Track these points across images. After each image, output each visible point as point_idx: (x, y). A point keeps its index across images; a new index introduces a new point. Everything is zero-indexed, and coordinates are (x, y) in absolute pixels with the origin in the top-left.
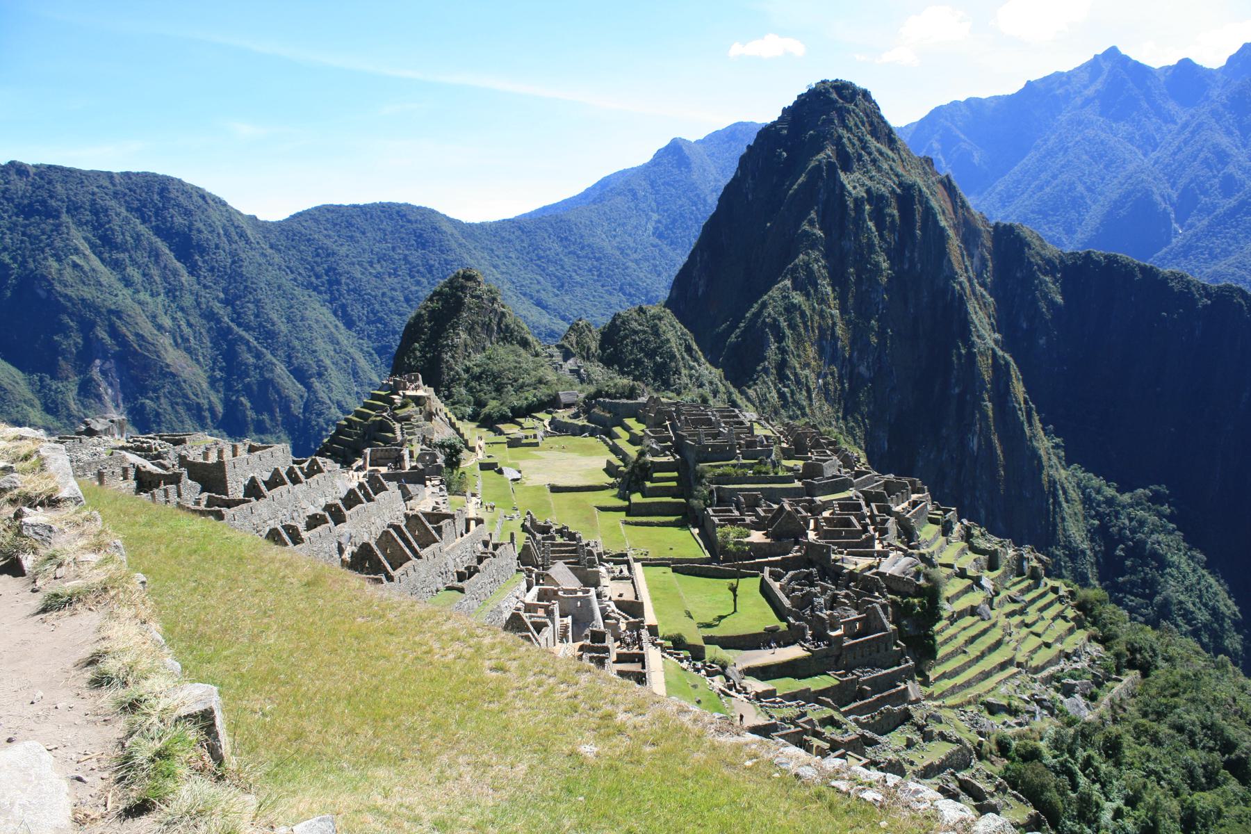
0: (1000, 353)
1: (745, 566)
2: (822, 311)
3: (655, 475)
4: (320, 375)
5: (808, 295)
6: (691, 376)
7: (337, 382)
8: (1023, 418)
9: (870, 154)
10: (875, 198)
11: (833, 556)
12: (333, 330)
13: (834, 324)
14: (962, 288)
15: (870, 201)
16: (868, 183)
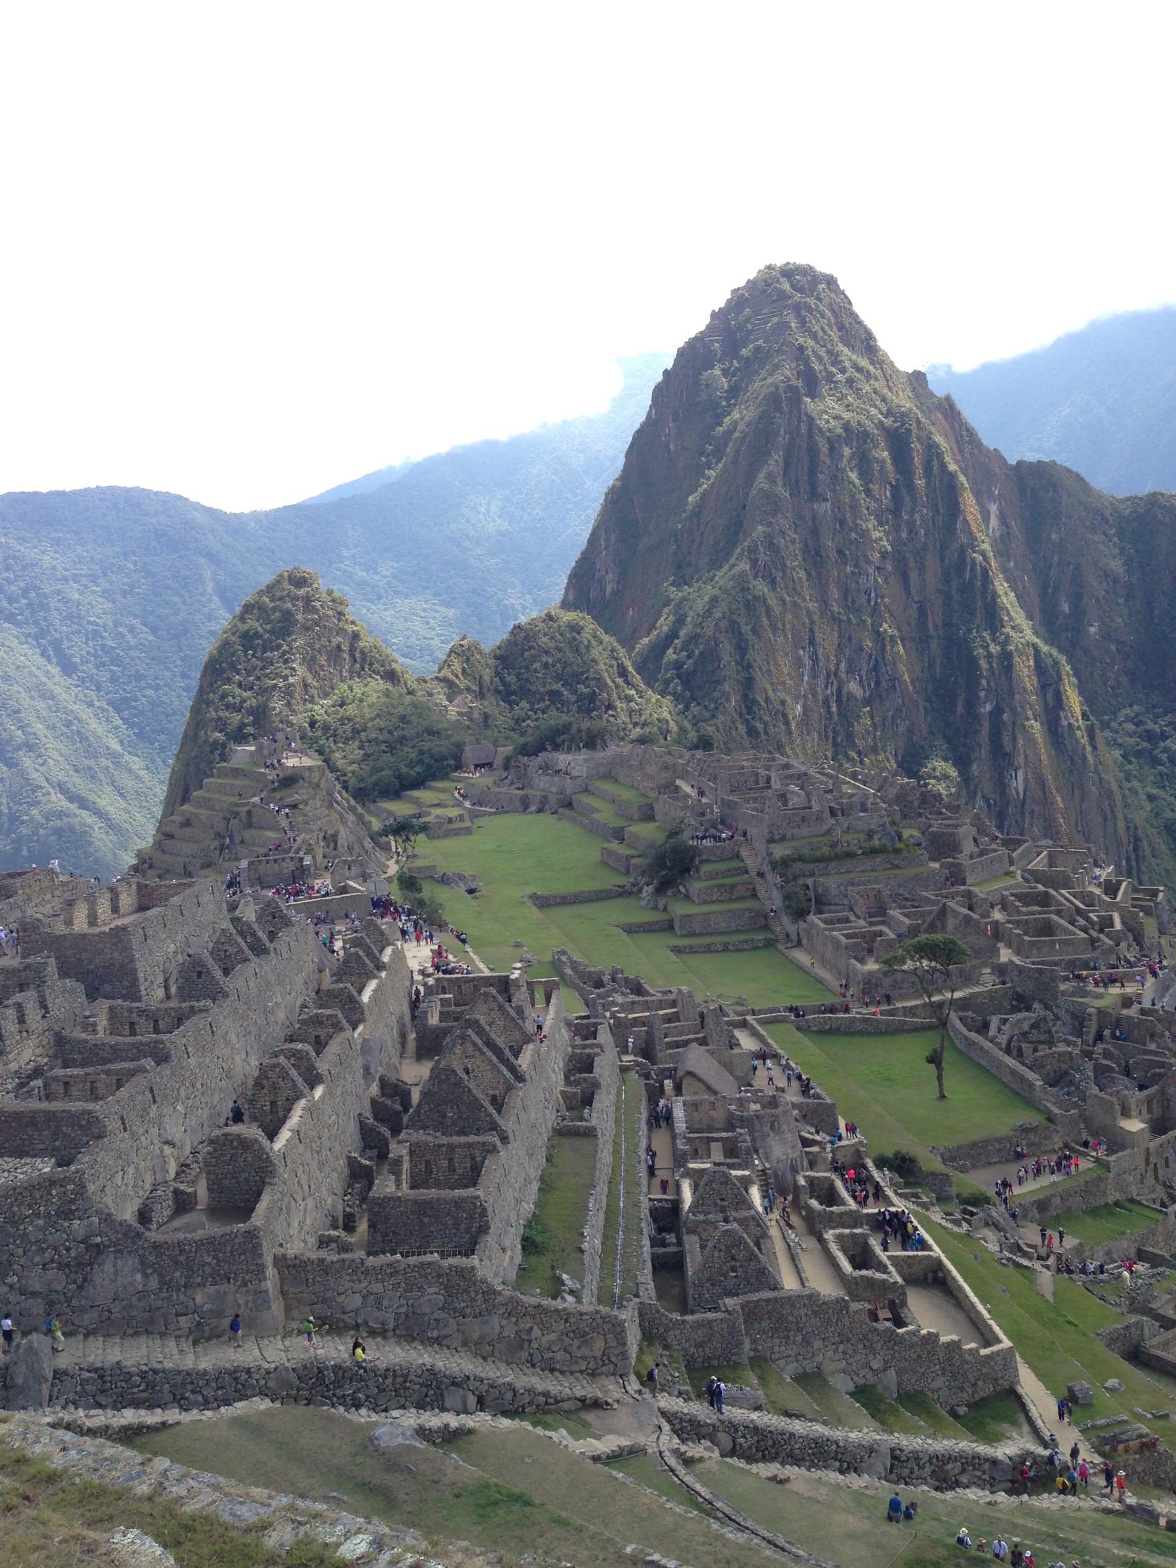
0: (1045, 648)
1: (911, 1011)
2: (795, 604)
3: (705, 868)
4: (30, 747)
5: (773, 583)
6: (631, 712)
7: (56, 756)
8: (1085, 741)
9: (843, 371)
10: (856, 436)
11: (1063, 987)
12: (44, 679)
13: (812, 622)
14: (985, 559)
15: (848, 441)
16: (847, 416)
